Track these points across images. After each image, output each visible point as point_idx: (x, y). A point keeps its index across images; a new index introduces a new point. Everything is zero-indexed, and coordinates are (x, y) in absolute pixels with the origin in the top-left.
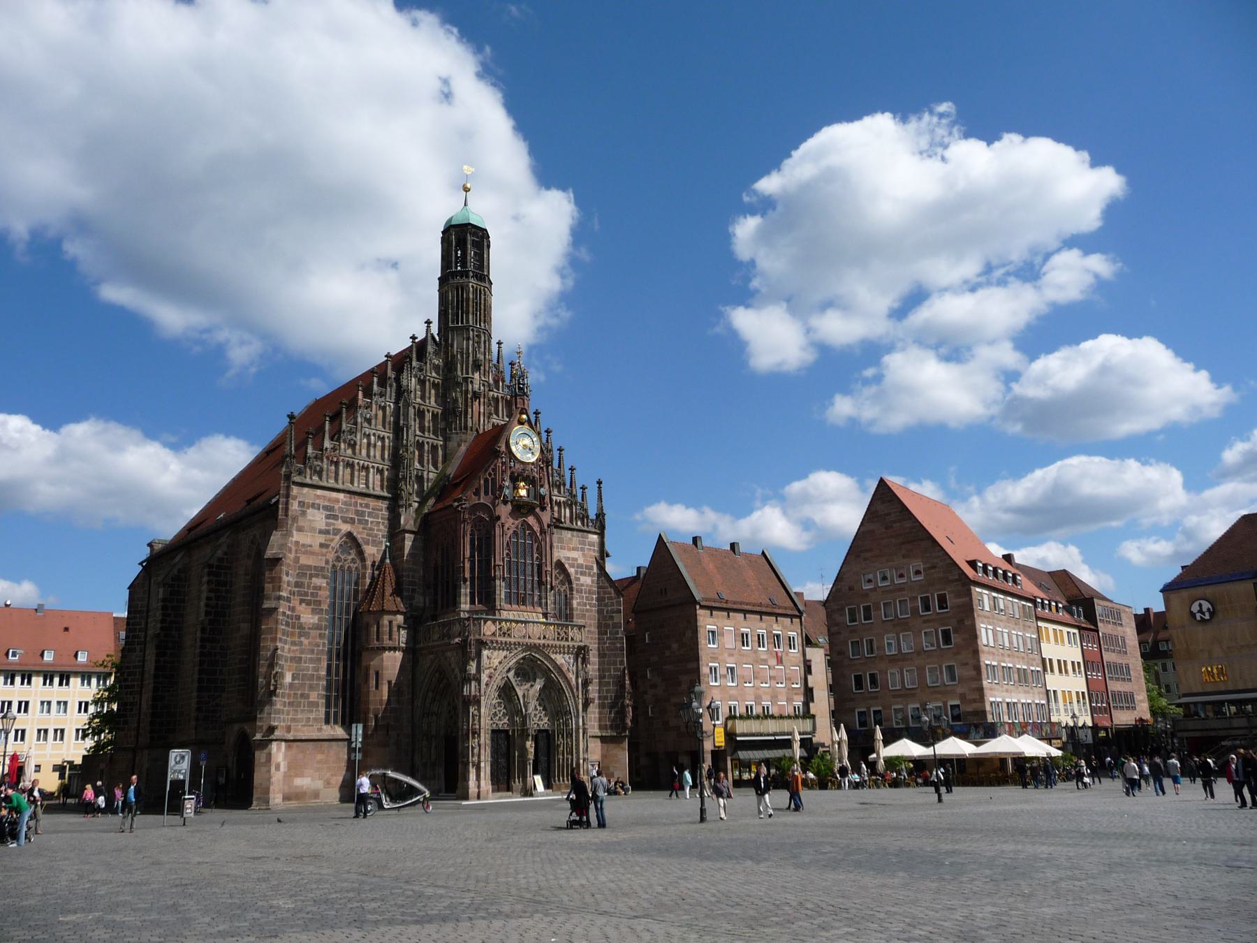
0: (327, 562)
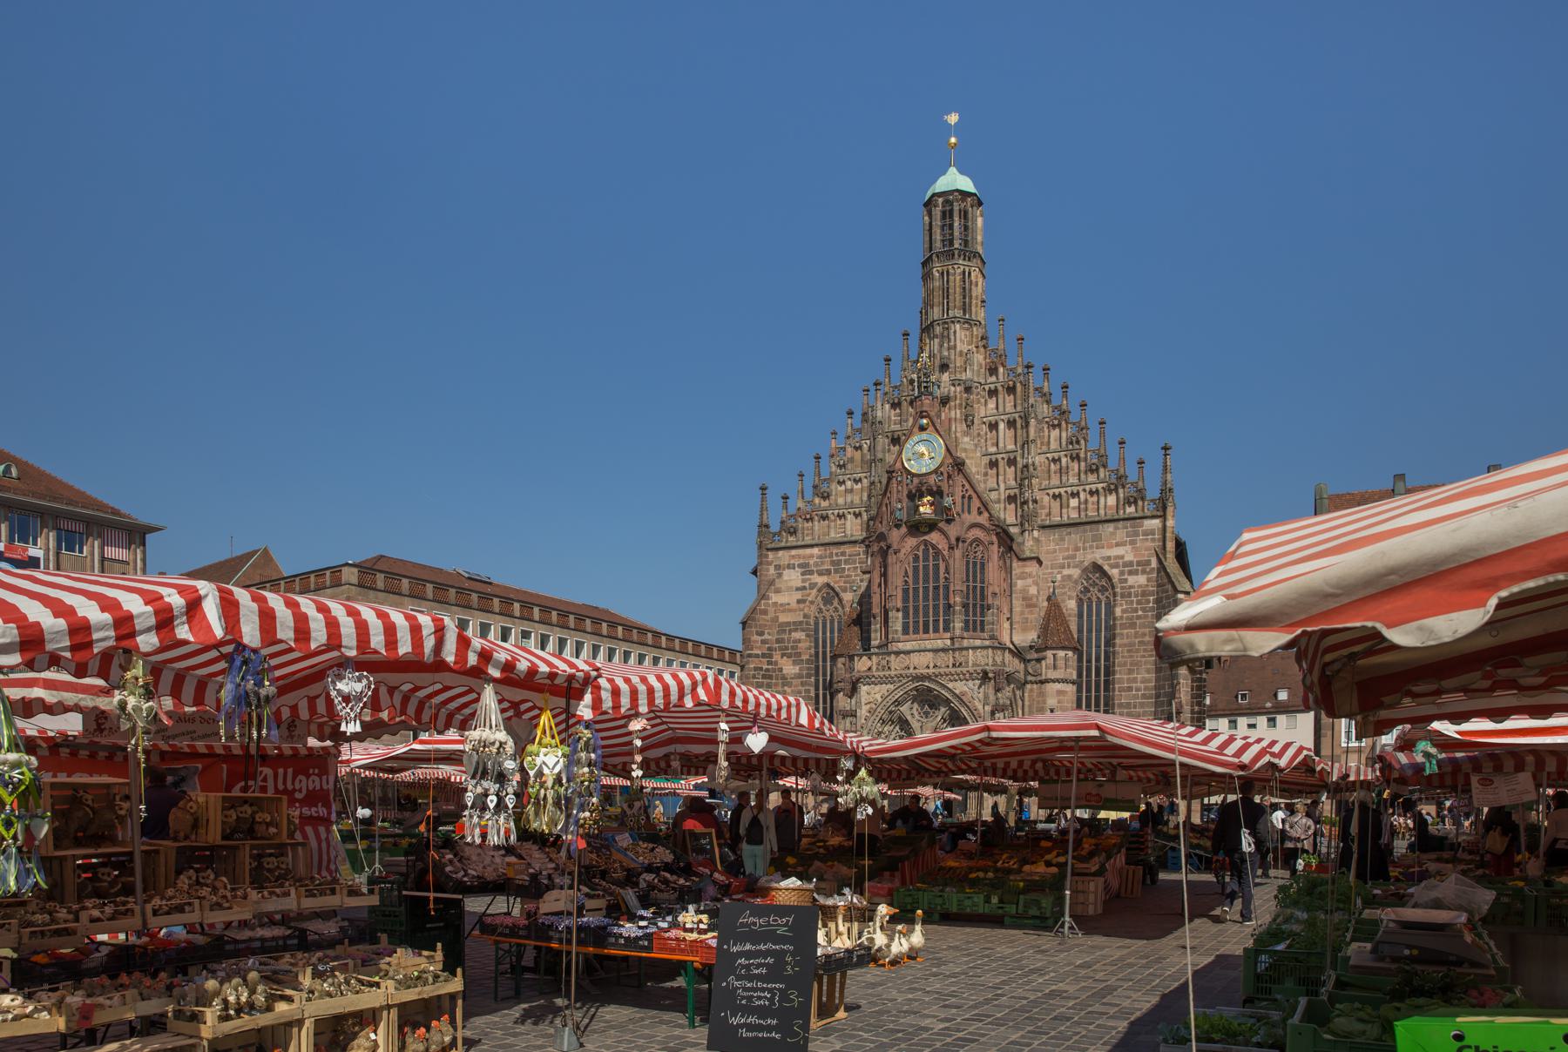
0: (805, 616)
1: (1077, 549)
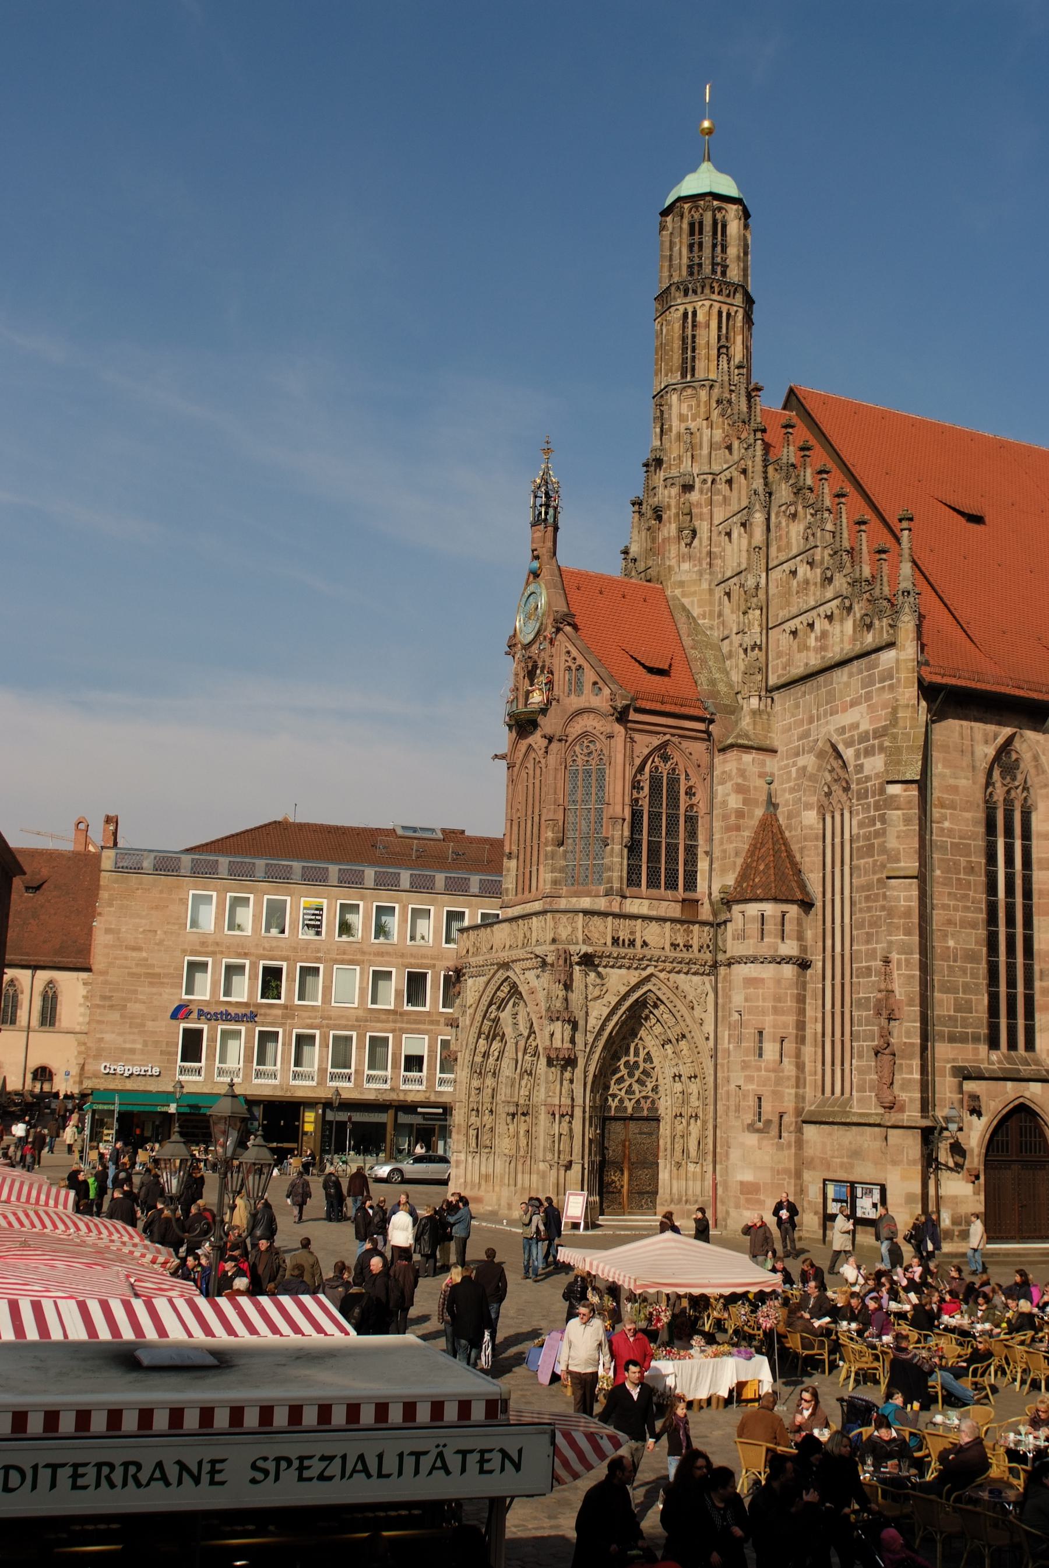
1: (811, 721)
